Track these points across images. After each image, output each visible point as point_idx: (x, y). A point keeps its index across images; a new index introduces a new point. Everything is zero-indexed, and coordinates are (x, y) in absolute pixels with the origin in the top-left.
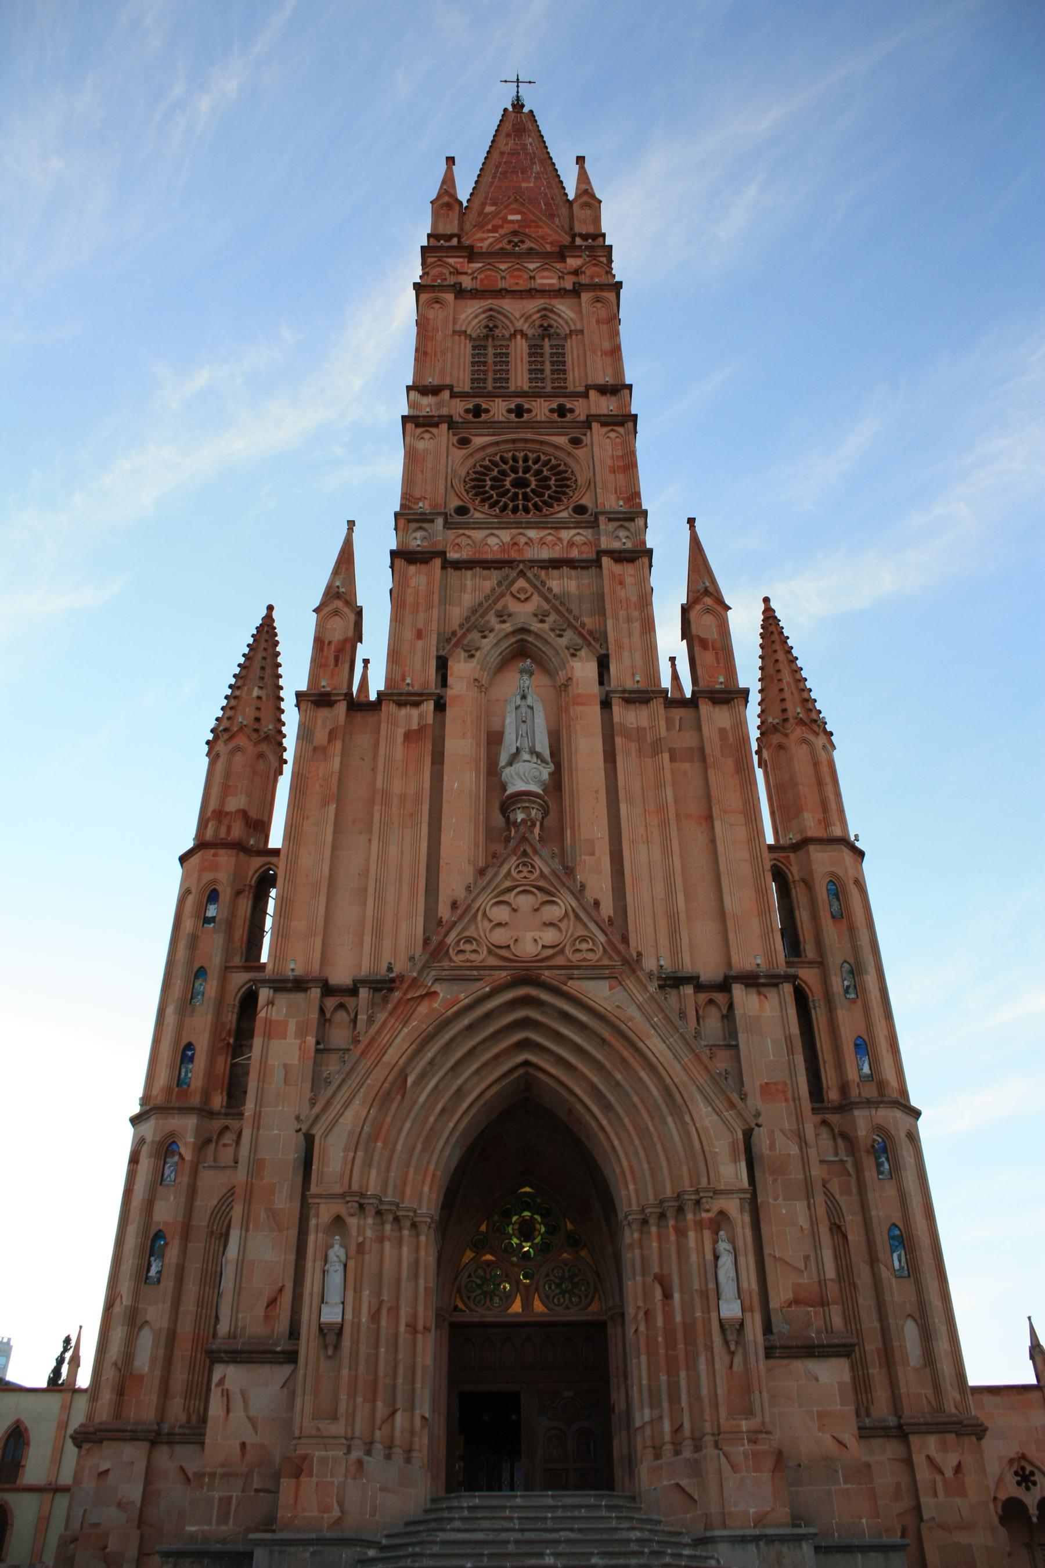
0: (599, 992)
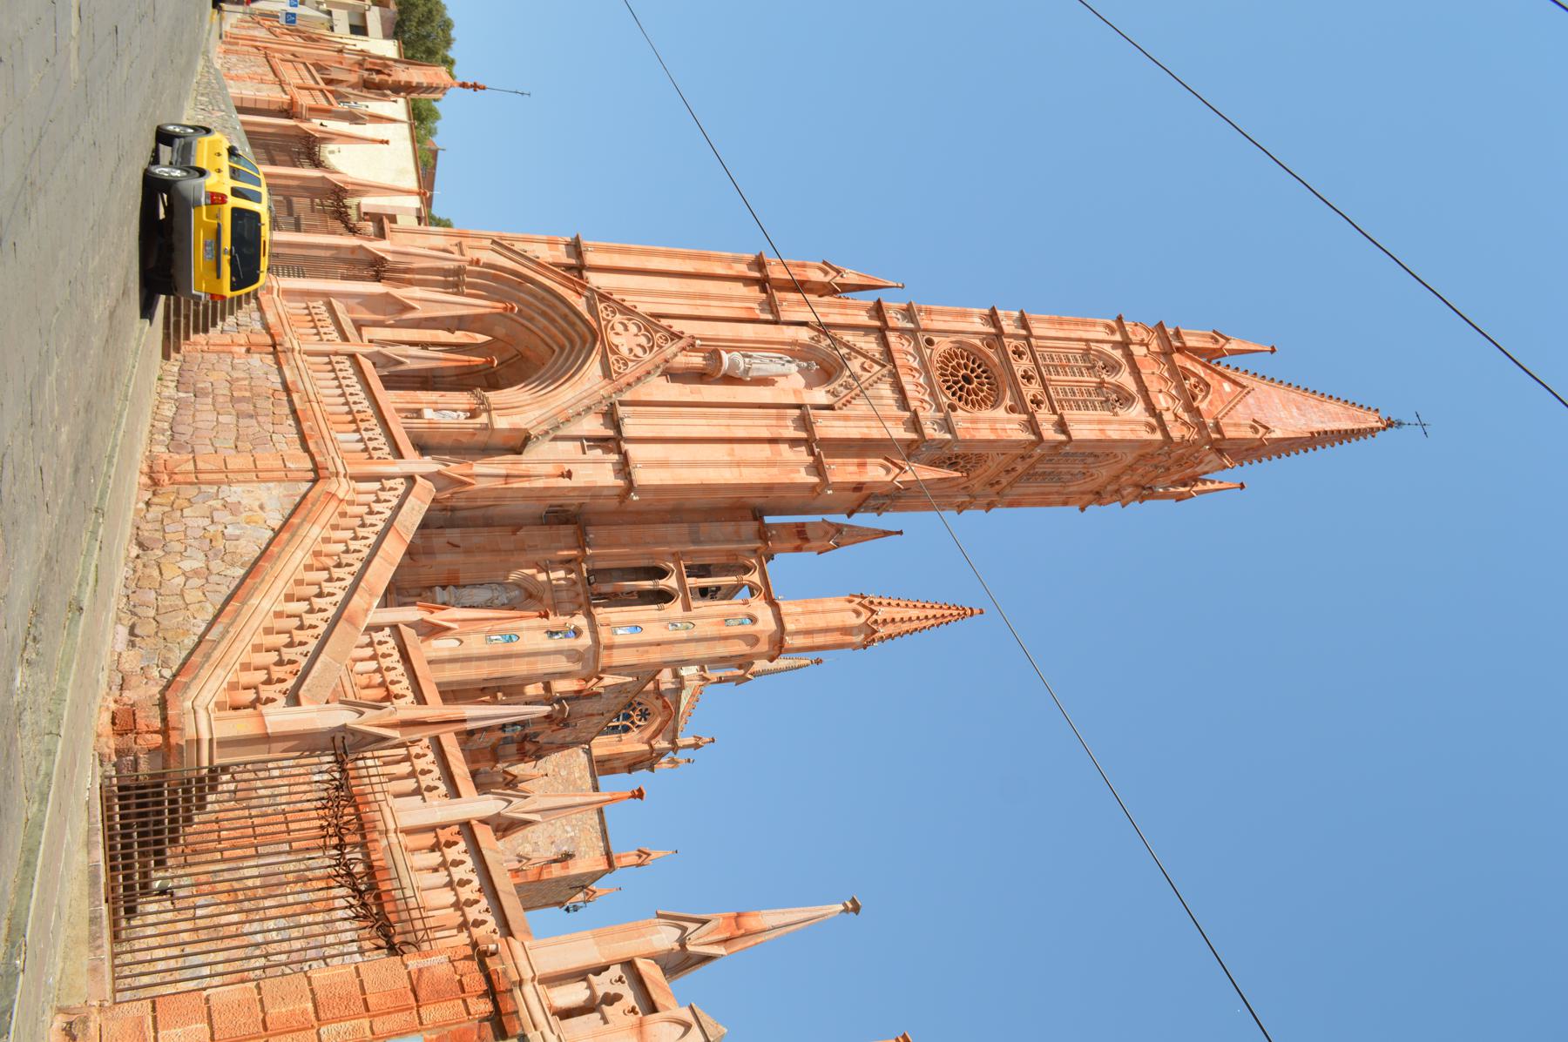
0: (593, 368)
